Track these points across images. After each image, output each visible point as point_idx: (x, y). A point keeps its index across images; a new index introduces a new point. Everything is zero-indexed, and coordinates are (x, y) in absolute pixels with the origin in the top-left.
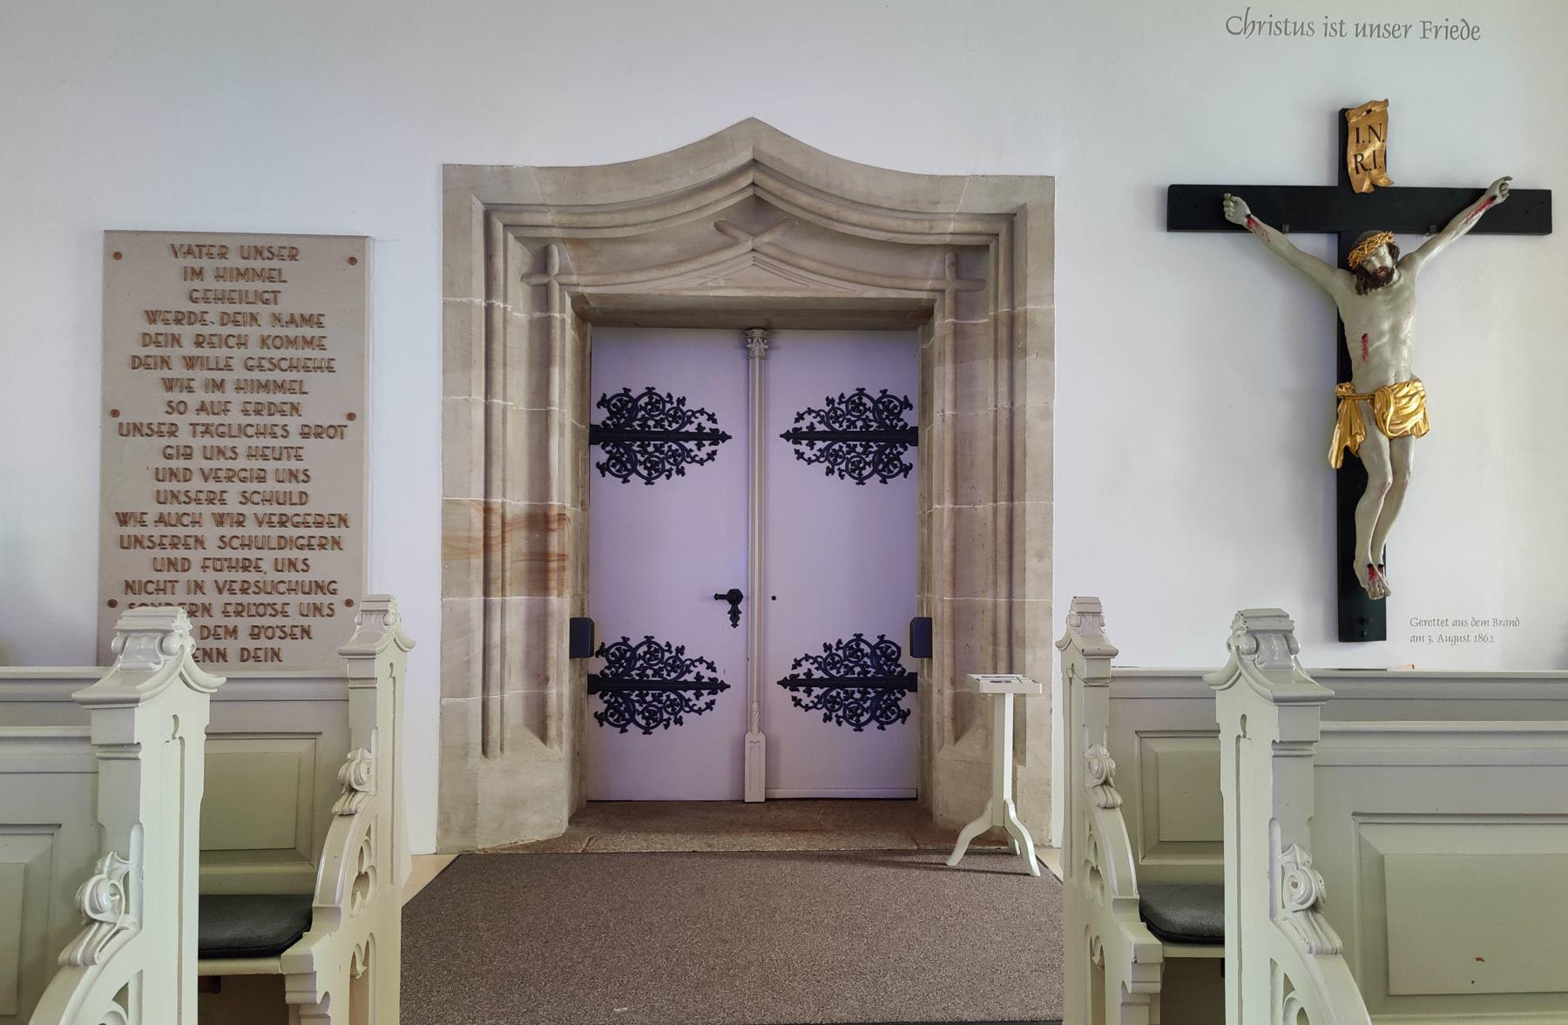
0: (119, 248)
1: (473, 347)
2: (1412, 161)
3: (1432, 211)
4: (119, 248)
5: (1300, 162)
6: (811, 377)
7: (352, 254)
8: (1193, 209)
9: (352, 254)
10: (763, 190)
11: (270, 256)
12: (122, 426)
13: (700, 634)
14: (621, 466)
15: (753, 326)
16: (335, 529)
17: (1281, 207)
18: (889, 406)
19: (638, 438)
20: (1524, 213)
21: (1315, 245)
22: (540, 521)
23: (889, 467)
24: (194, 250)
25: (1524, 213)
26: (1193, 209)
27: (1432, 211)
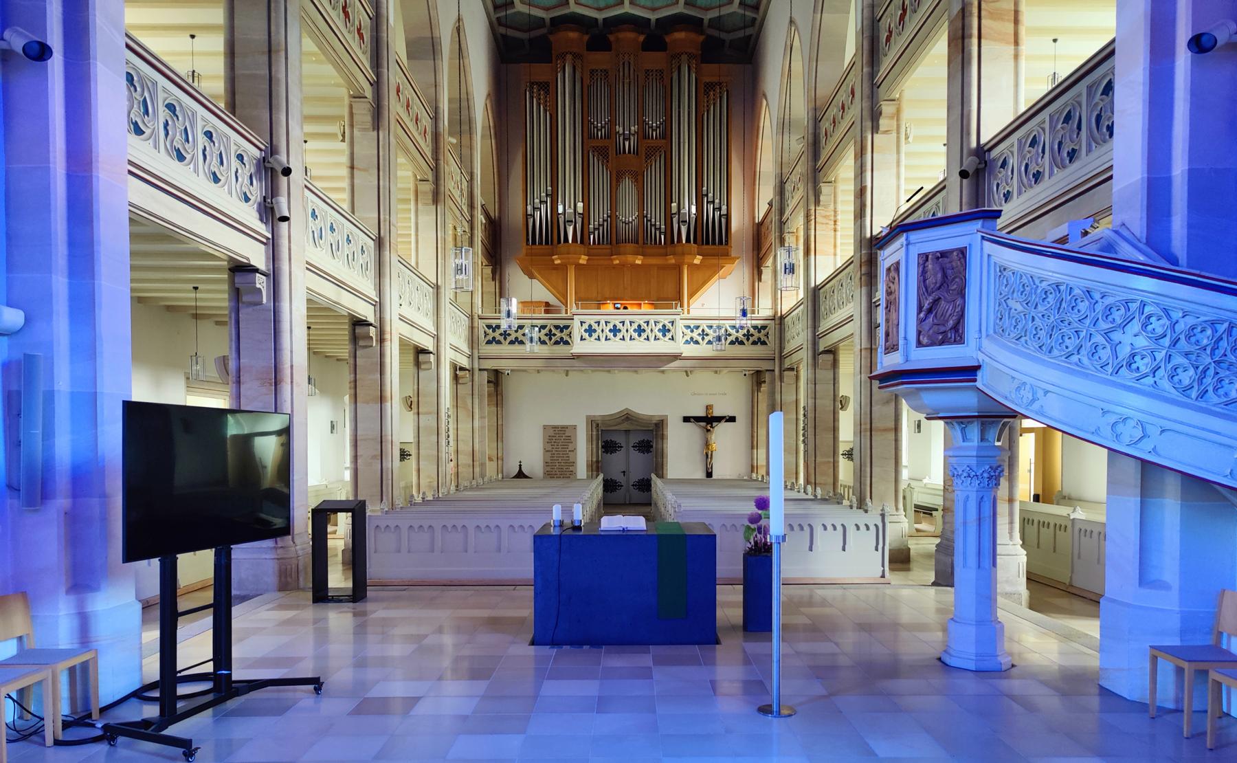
0: (545, 427)
1: (590, 439)
2: (716, 413)
3: (719, 419)
4: (545, 427)
5: (702, 413)
6: (634, 439)
7: (575, 427)
8: (686, 419)
9: (575, 427)
10: (627, 417)
11: (564, 428)
12: (546, 451)
13: (620, 478)
14: (606, 452)
15: (627, 432)
16: (573, 463)
17: (698, 419)
18: (649, 442)
19: (610, 448)
20: (732, 419)
21: (703, 424)
22: (597, 462)
23: (649, 452)
24: (555, 427)
25: (732, 419)
26: (686, 419)
27: (719, 419)
